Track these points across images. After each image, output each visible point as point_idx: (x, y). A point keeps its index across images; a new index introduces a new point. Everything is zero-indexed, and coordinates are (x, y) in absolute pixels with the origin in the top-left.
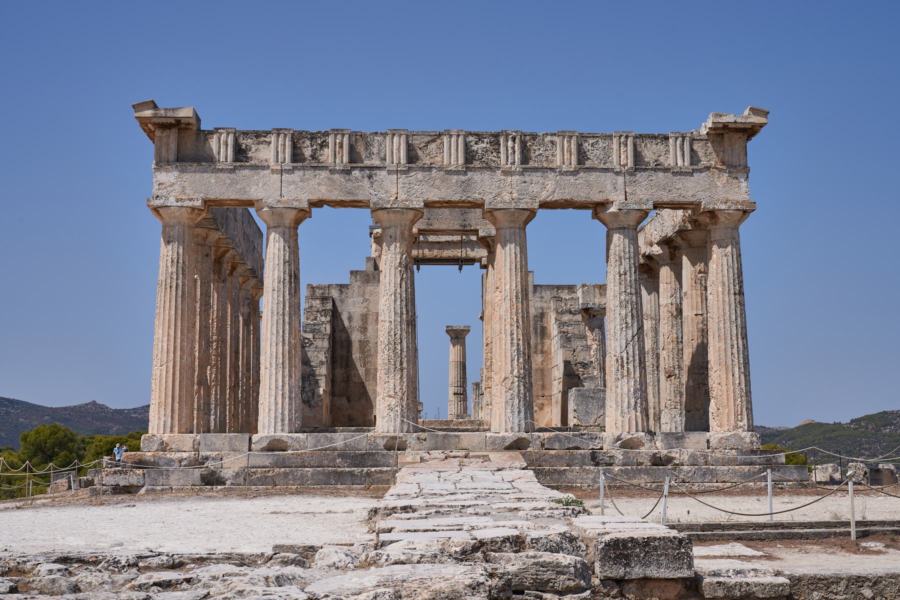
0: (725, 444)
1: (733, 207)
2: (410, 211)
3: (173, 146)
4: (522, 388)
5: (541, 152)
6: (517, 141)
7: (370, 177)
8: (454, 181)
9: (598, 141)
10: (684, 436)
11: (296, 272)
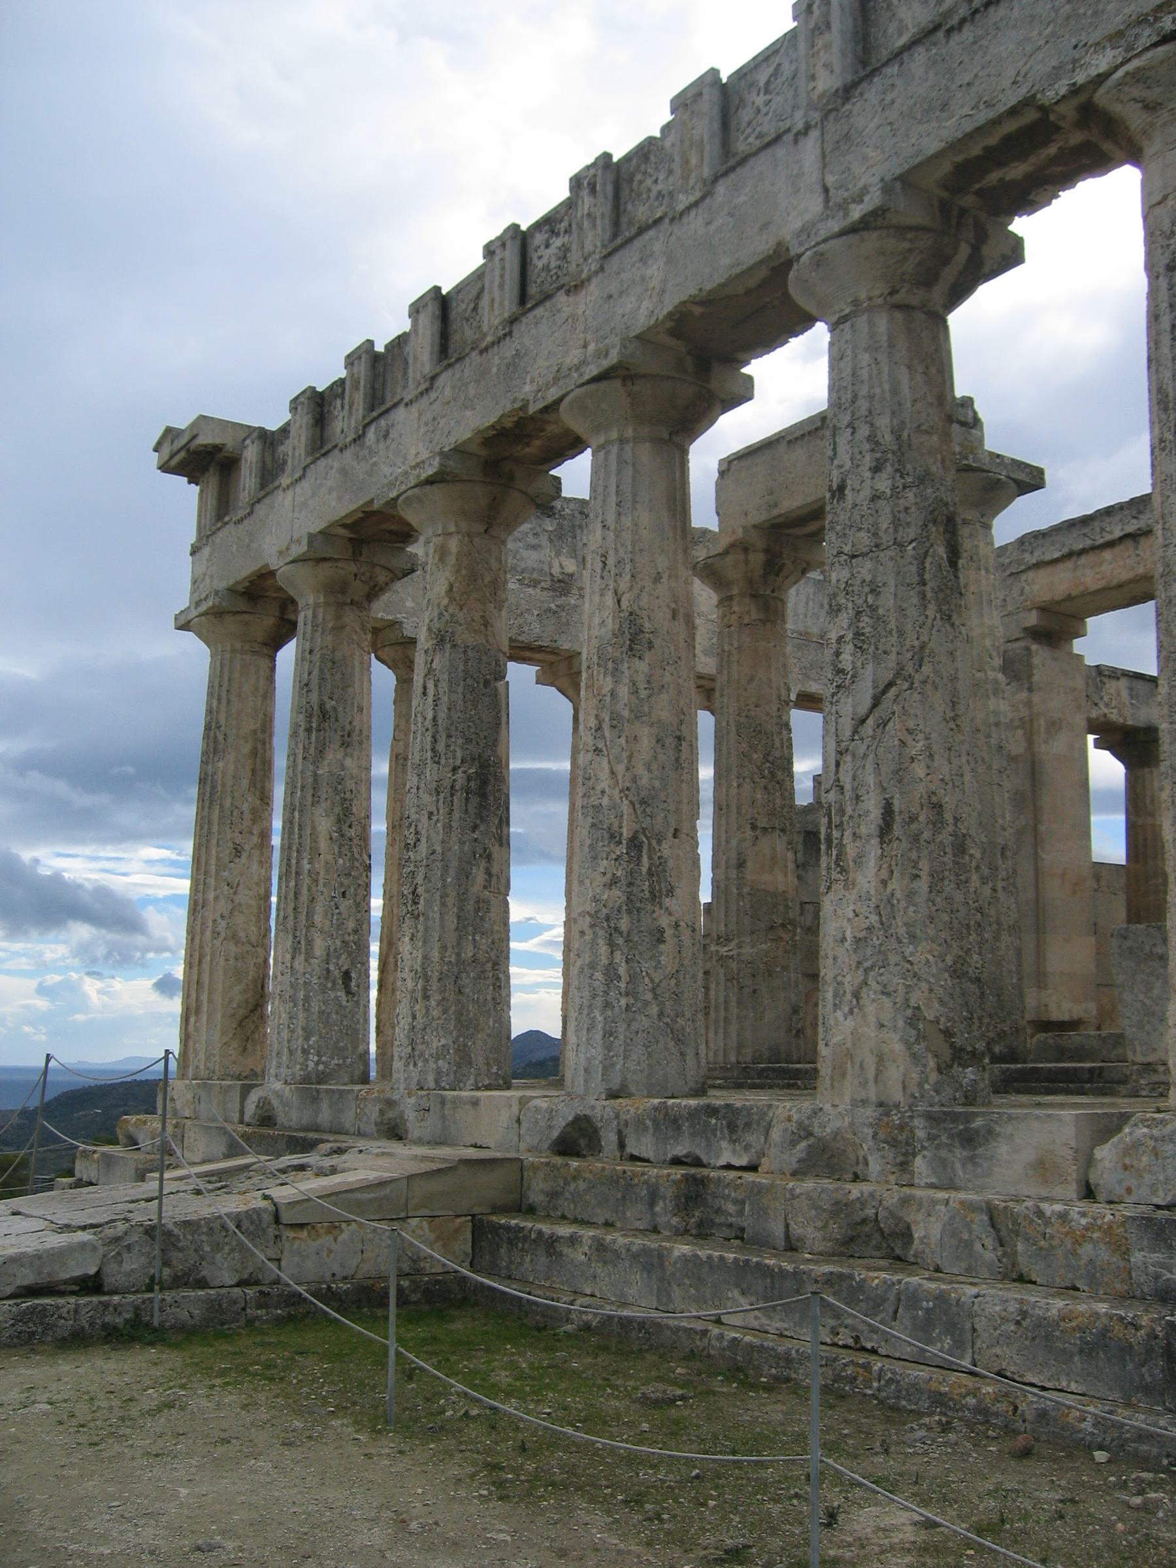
0: (1148, 1178)
1: (1147, 36)
2: (428, 488)
3: (212, 502)
4: (603, 949)
5: (660, 187)
6: (598, 188)
7: (386, 436)
8: (495, 370)
9: (779, 65)
10: (990, 1132)
11: (330, 704)
